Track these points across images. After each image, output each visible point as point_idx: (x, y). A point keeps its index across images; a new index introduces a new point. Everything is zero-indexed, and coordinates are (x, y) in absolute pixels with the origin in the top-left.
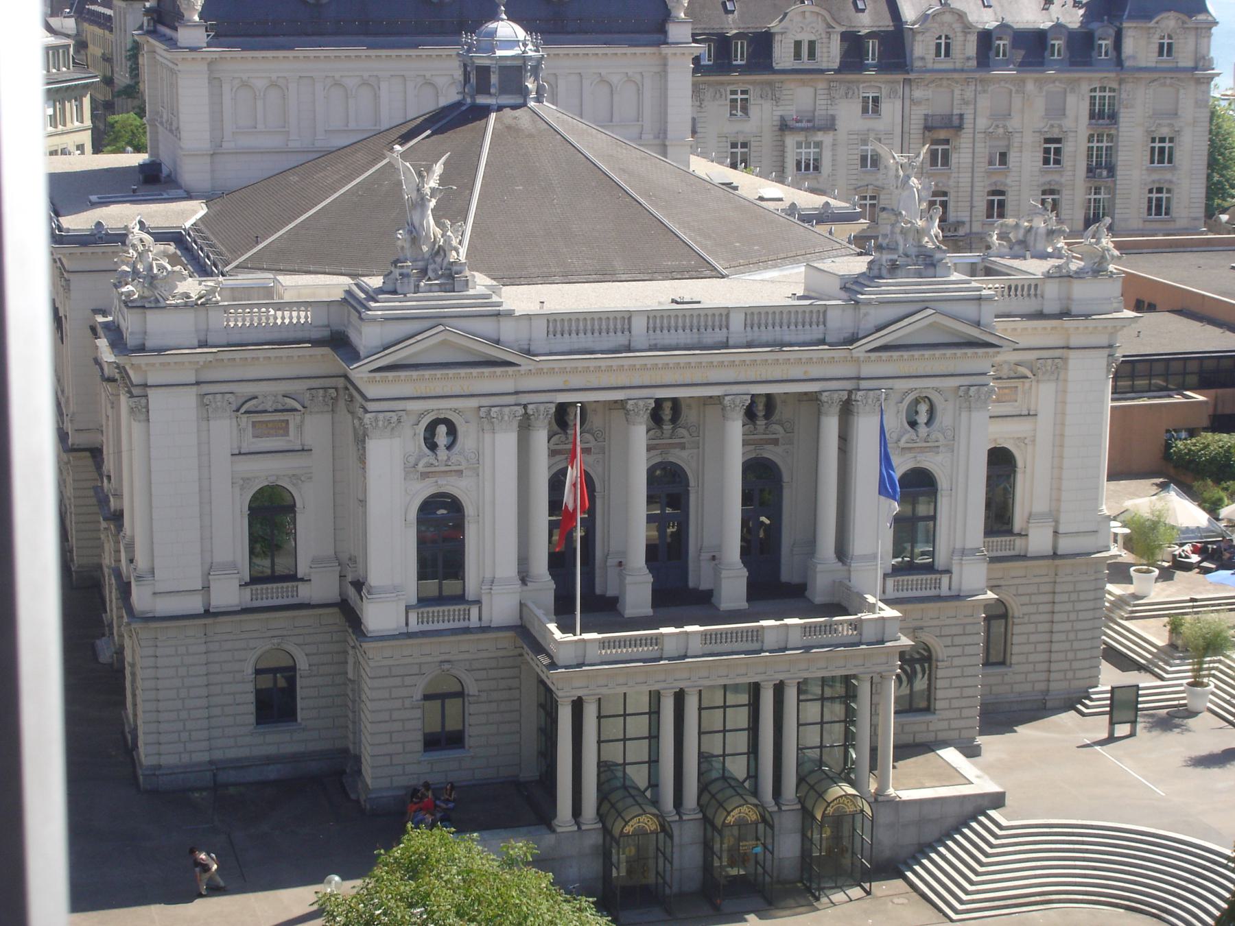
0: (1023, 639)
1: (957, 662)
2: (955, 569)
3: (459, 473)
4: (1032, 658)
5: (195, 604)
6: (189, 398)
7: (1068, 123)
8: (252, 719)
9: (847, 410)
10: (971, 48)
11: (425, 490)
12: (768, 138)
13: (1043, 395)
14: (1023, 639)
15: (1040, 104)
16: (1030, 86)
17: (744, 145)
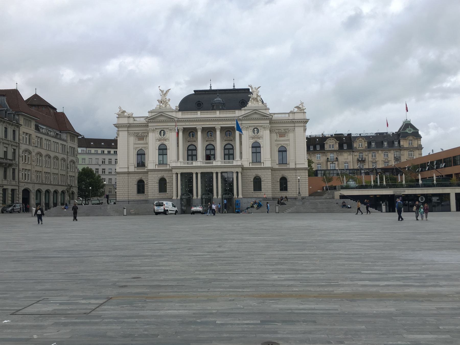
0: (290, 185)
1: (266, 181)
2: (264, 162)
3: (166, 140)
4: (292, 189)
5: (126, 170)
6: (126, 133)
7: (389, 159)
8: (136, 192)
9: (239, 130)
10: (366, 145)
11: (159, 143)
12: (325, 163)
13: (291, 135)
14: (290, 185)
15: (383, 155)
16: (380, 152)
17: (320, 164)
